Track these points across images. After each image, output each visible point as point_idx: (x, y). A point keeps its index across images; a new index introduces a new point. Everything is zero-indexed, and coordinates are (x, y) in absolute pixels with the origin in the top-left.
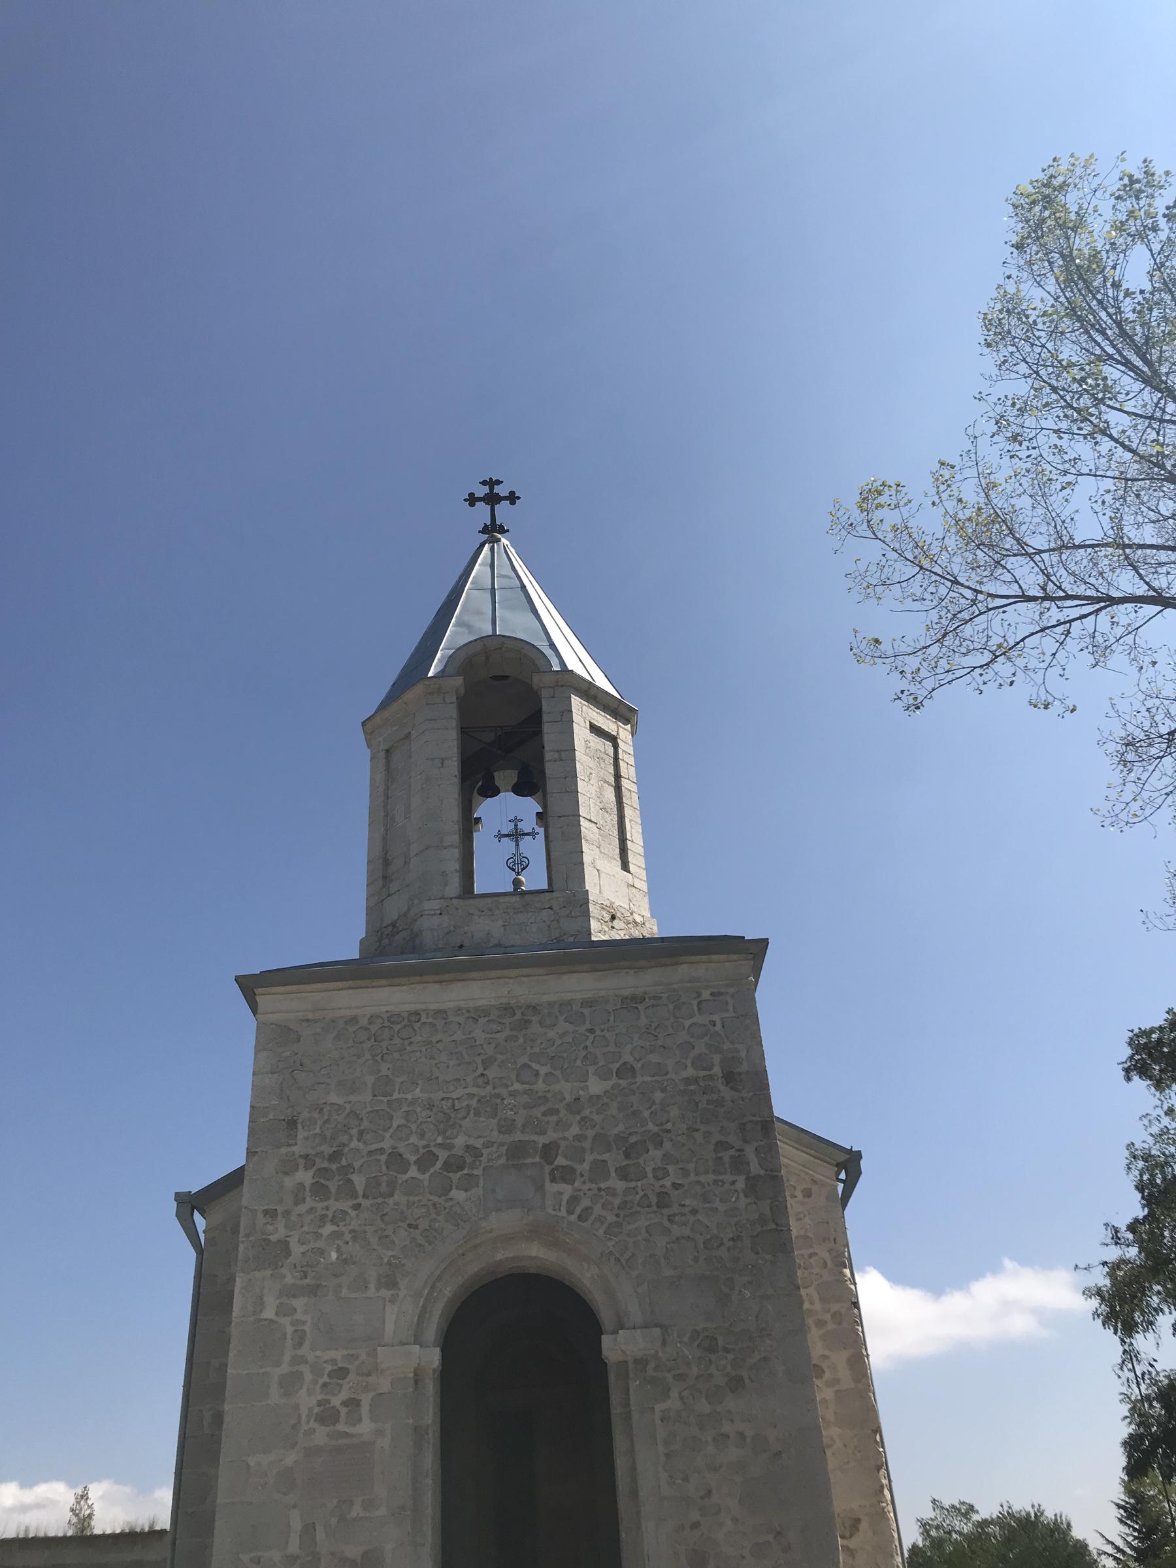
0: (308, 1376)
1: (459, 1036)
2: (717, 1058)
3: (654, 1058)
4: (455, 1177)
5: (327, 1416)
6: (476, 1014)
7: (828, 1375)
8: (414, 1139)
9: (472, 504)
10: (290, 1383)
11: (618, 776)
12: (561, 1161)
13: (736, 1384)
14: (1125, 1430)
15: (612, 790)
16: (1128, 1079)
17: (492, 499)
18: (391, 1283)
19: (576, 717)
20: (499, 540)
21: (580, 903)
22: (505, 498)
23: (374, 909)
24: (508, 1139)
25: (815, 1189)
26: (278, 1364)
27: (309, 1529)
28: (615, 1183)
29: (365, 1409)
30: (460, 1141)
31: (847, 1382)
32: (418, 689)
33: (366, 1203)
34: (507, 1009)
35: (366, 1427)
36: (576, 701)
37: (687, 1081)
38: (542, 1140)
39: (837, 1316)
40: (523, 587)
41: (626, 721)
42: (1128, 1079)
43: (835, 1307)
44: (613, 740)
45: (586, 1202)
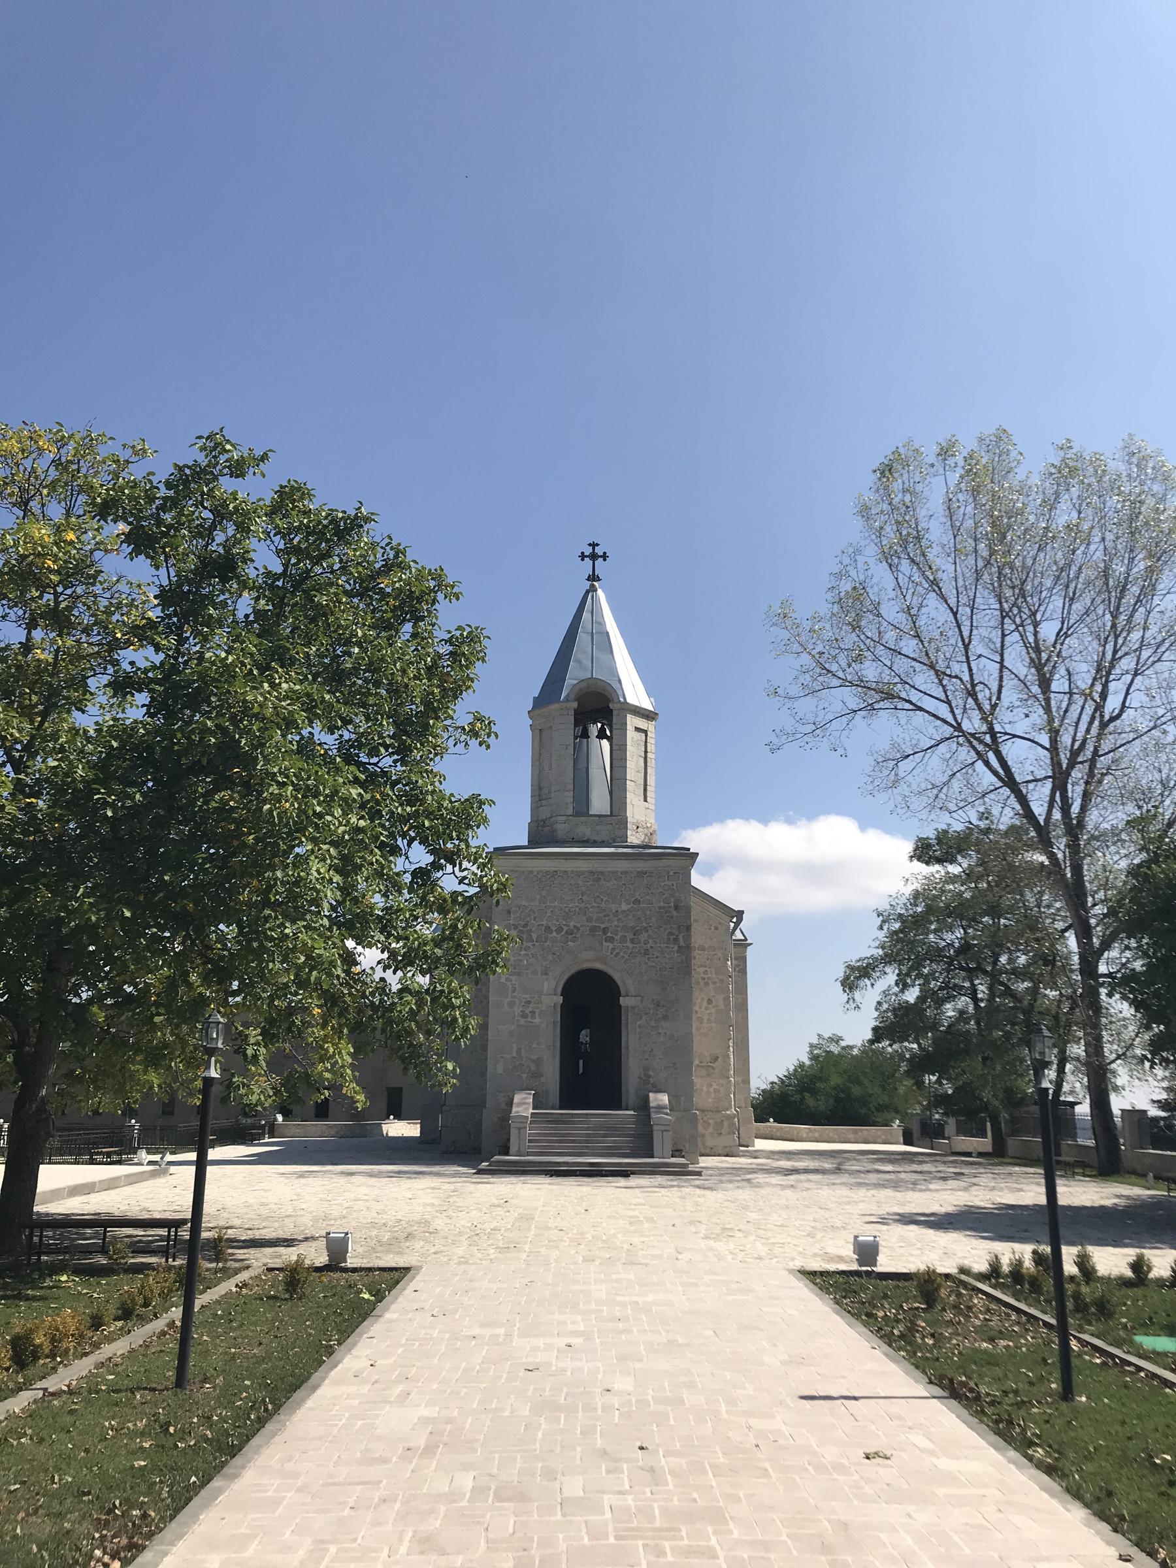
0: (517, 1003)
1: (572, 882)
2: (673, 899)
3: (648, 897)
4: (570, 937)
5: (524, 1016)
6: (579, 874)
7: (714, 1004)
8: (555, 922)
9: (583, 560)
10: (511, 1004)
11: (646, 752)
12: (609, 934)
13: (665, 1018)
14: (873, 1023)
15: (643, 760)
16: (911, 861)
17: (594, 557)
18: (547, 974)
19: (630, 728)
20: (596, 590)
21: (623, 823)
22: (601, 556)
23: (535, 809)
24: (590, 924)
25: (720, 926)
26: (507, 997)
27: (519, 1050)
28: (628, 944)
29: (537, 1015)
30: (572, 924)
31: (722, 1007)
32: (556, 706)
33: (537, 944)
34: (591, 872)
35: (537, 1020)
36: (629, 717)
37: (660, 908)
38: (603, 926)
39: (722, 981)
40: (608, 633)
41: (653, 719)
42: (911, 861)
43: (721, 977)
44: (645, 732)
45: (617, 951)
